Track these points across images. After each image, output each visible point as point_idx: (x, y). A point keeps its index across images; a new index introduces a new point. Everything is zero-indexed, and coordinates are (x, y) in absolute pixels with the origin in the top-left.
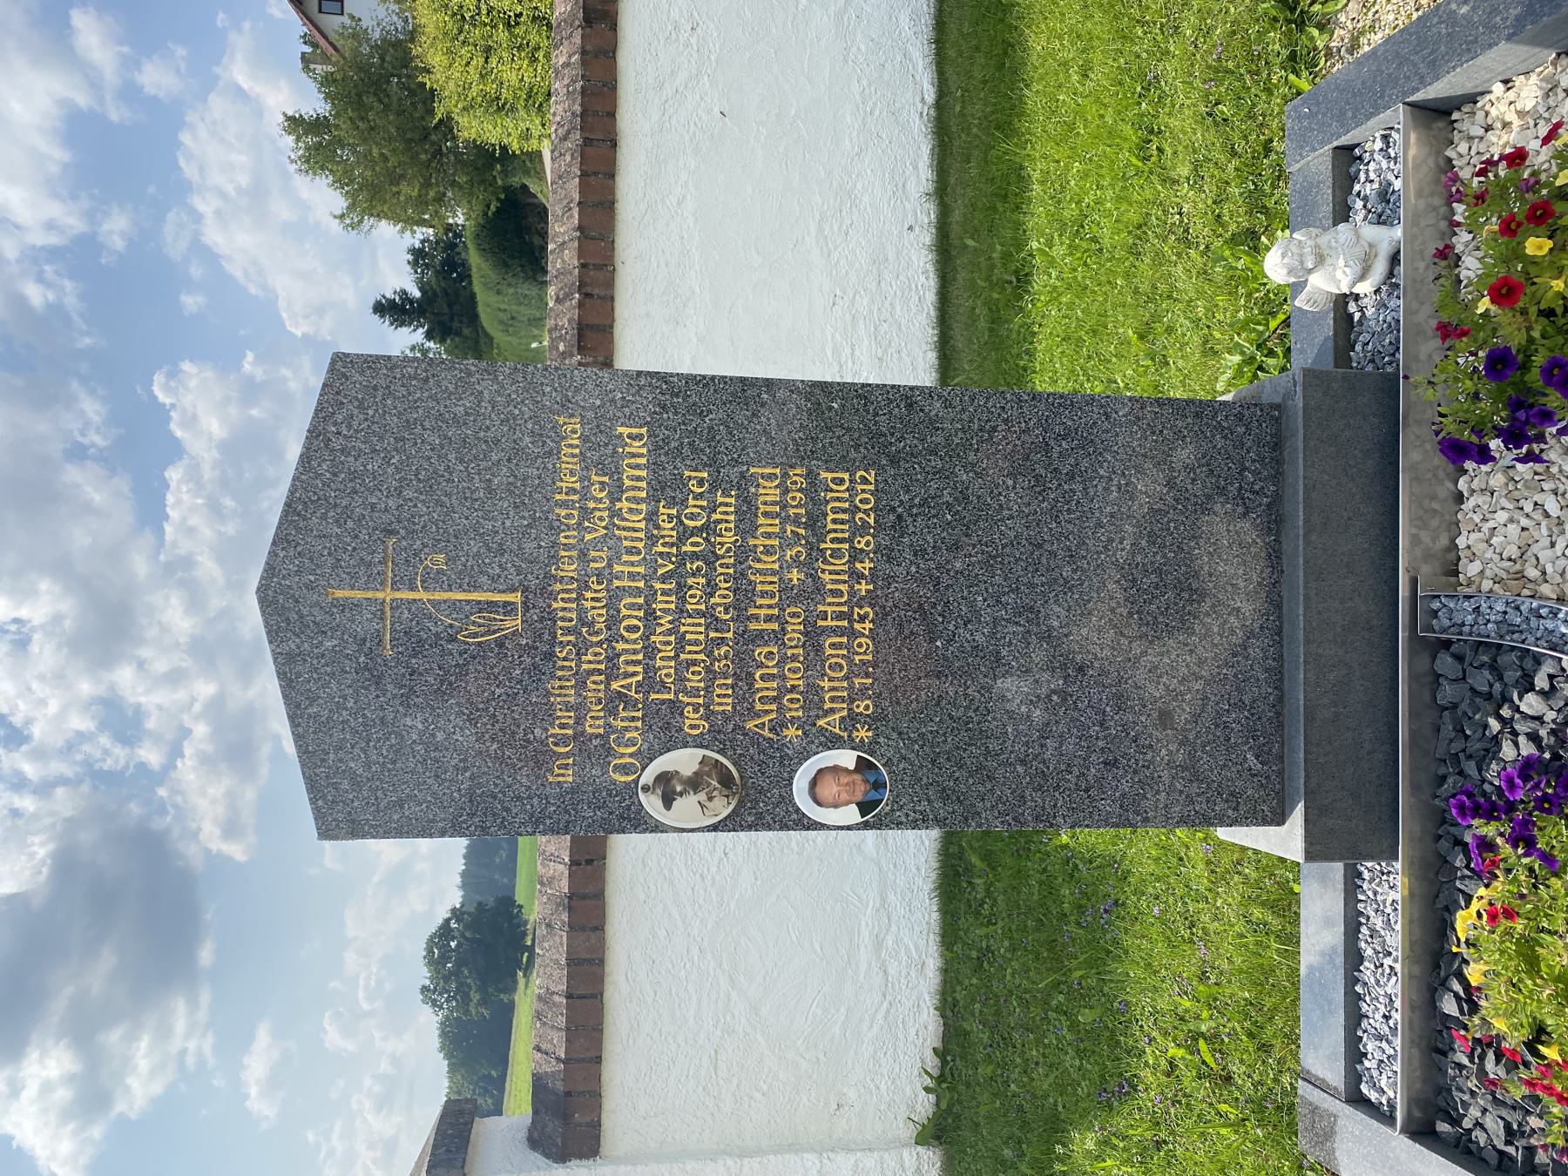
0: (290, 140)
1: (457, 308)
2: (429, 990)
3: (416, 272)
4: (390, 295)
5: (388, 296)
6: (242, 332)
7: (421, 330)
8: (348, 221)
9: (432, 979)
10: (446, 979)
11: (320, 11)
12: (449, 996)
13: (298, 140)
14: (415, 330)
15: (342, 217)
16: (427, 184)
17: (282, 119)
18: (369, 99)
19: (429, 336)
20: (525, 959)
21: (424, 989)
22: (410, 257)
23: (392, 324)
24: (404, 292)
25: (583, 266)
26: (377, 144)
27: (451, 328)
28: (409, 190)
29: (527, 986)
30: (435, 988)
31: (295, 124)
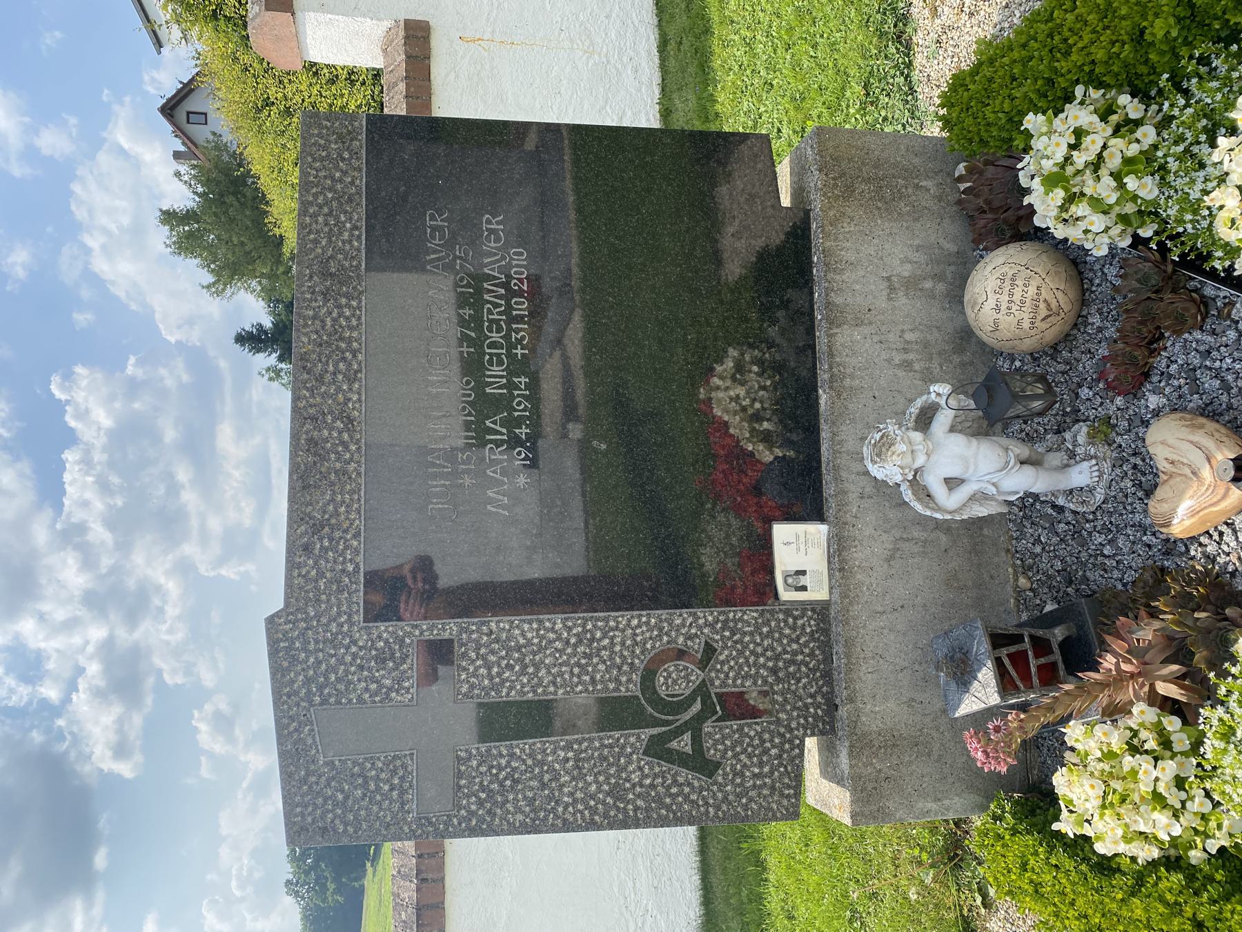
2: (292, 884)
3: (269, 306)
5: (247, 329)
6: (120, 503)
7: (274, 355)
8: (214, 290)
9: (294, 874)
10: (307, 873)
11: (188, 122)
12: (309, 887)
13: (172, 230)
15: (208, 287)
17: (159, 213)
18: (230, 199)
20: (372, 852)
21: (288, 883)
23: (250, 351)
25: (420, 856)
29: (374, 875)
30: (297, 882)
31: (169, 217)
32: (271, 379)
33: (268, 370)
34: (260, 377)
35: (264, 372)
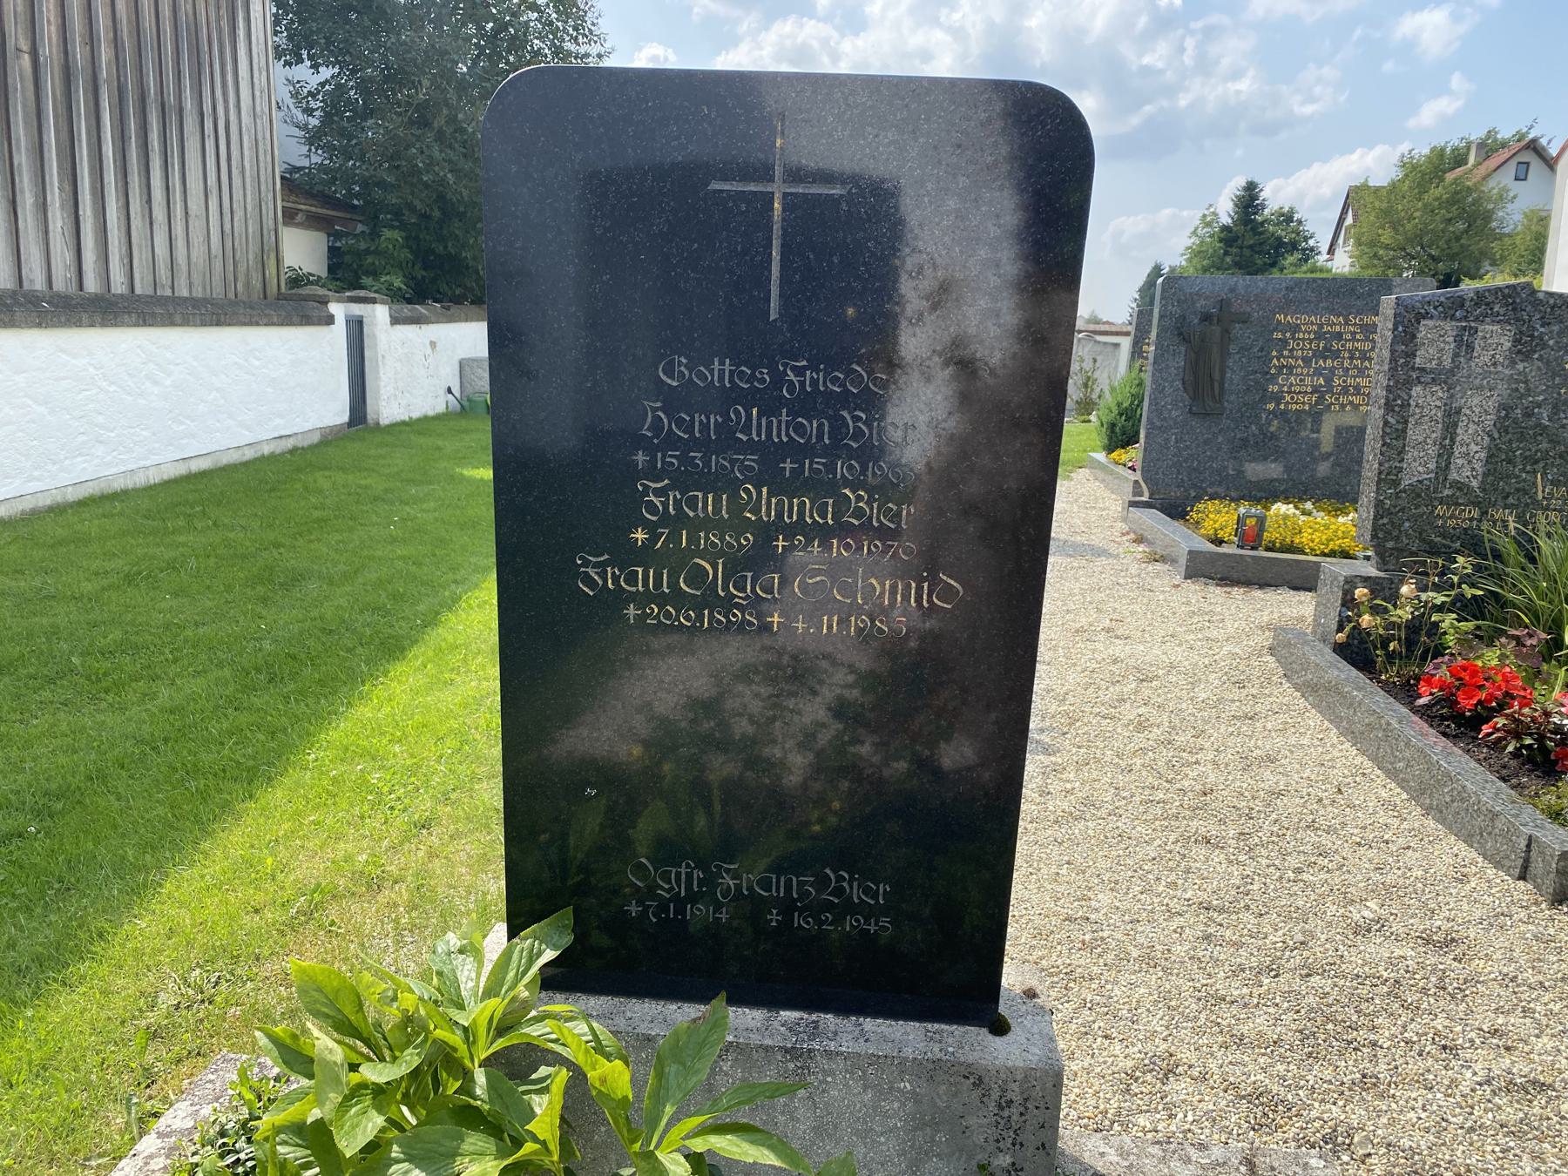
0: (1426, 151)
1: (1247, 252)
3: (1273, 214)
4: (1263, 195)
5: (1262, 194)
7: (1230, 221)
14: (1230, 215)
16: (1387, 247)
19: (1225, 228)
22: (1286, 209)
24: (1263, 209)
26: (1422, 216)
27: (1231, 246)
28: (1387, 236)
32: (1204, 216)
33: (1214, 214)
34: (1207, 206)
35: (1212, 210)
